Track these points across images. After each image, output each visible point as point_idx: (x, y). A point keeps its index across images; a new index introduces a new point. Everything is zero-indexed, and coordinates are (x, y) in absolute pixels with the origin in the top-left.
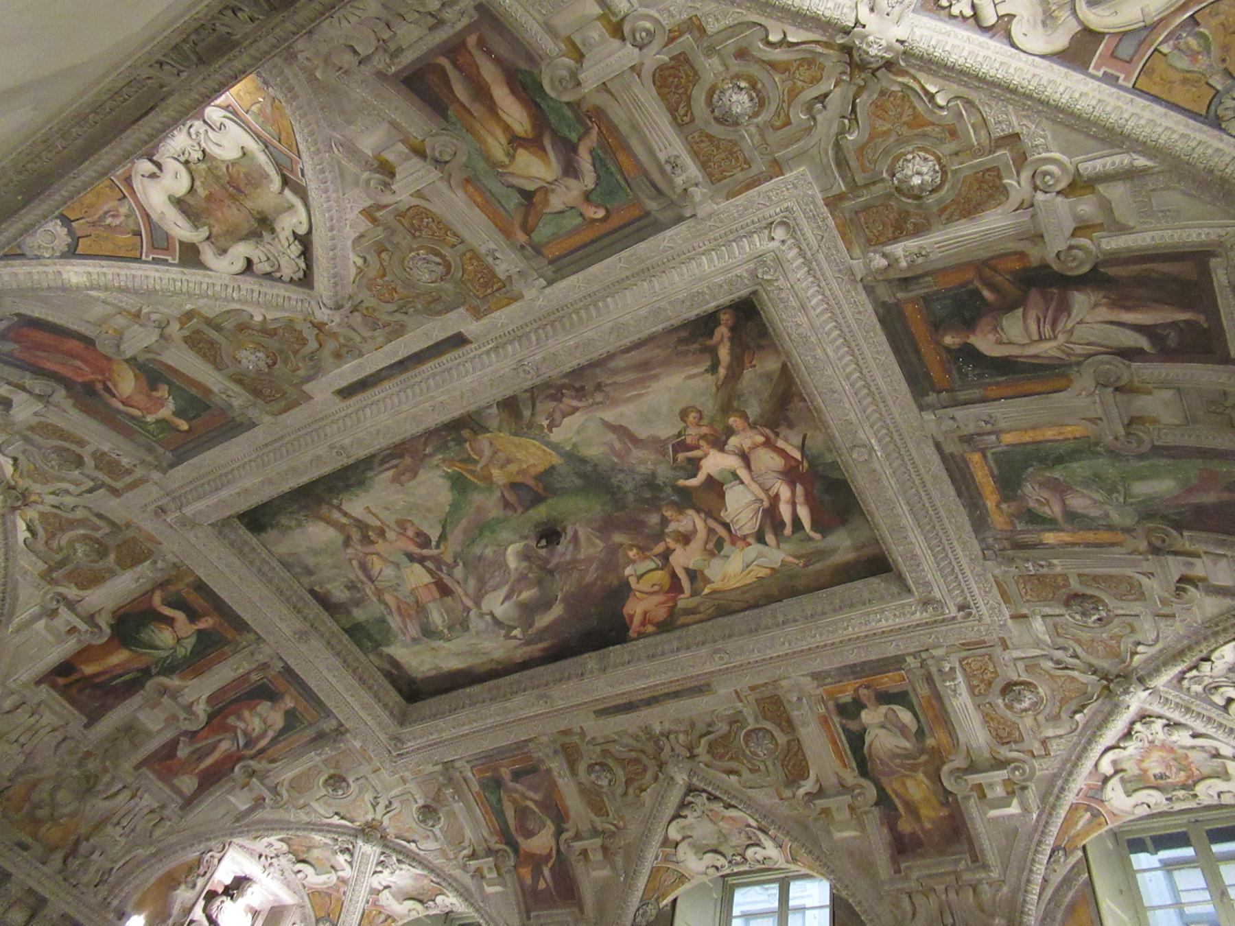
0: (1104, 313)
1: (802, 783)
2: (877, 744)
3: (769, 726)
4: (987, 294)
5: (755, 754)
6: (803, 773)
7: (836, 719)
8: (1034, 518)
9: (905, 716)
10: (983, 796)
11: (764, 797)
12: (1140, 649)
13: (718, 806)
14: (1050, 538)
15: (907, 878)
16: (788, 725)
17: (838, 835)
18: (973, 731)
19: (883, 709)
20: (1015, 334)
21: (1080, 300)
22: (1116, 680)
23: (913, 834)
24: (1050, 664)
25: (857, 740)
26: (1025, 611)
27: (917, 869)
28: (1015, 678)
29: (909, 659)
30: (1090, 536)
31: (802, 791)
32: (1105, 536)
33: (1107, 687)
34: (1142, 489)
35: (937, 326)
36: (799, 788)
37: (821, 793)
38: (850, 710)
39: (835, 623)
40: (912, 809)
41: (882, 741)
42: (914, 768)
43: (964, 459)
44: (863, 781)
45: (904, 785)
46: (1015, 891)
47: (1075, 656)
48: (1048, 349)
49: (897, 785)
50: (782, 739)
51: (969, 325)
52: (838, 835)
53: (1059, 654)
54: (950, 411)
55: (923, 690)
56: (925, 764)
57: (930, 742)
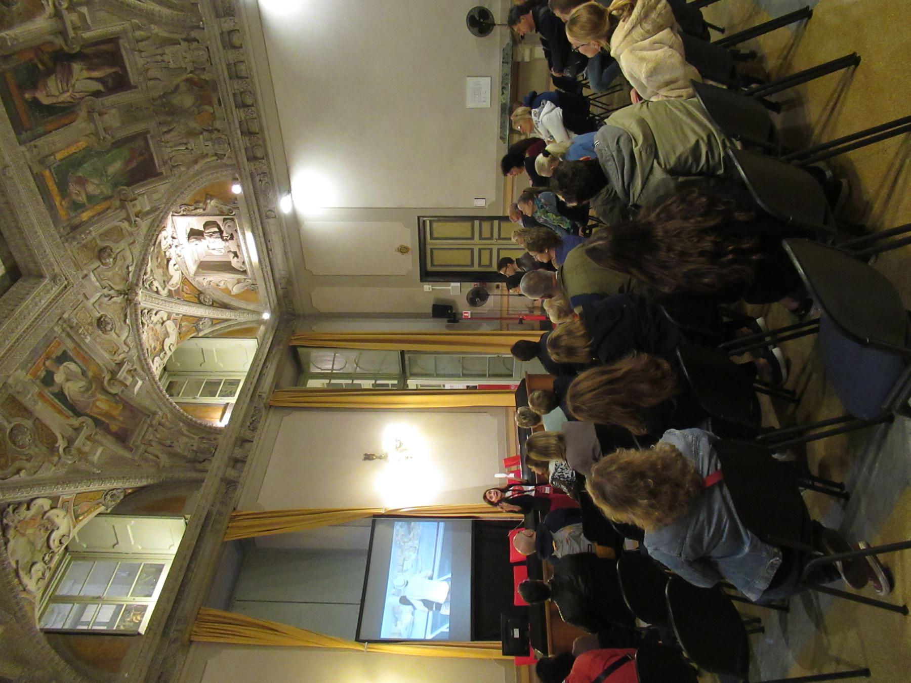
0: (86, 74)
1: (57, 445)
2: (72, 393)
3: (17, 421)
4: (40, 66)
5: (23, 447)
6: (56, 441)
7: (46, 391)
8: (77, 207)
9: (72, 366)
10: (126, 386)
11: (48, 472)
12: (130, 269)
13: (24, 513)
14: (85, 216)
15: (137, 447)
16: (25, 411)
17: (95, 458)
18: (103, 357)
19: (61, 368)
20: (52, 92)
21: (76, 67)
22: (128, 293)
23: (120, 428)
24: (107, 299)
25: (61, 396)
26: (85, 272)
27: (136, 439)
28: (99, 315)
29: (56, 329)
30: (98, 208)
31: (61, 450)
32: (104, 205)
33: (127, 299)
34: (111, 170)
35: (22, 87)
36: (58, 450)
37: (70, 442)
38: (48, 380)
39: (21, 312)
40: (108, 415)
41: (73, 389)
42: (93, 395)
43: (42, 175)
44: (81, 419)
45: (97, 406)
46: (171, 411)
47: (112, 288)
48: (65, 97)
49: (96, 410)
50: (28, 423)
51: (35, 87)
52: (95, 458)
53: (106, 291)
54: (32, 143)
55: (69, 345)
56: (96, 389)
57: (90, 374)
